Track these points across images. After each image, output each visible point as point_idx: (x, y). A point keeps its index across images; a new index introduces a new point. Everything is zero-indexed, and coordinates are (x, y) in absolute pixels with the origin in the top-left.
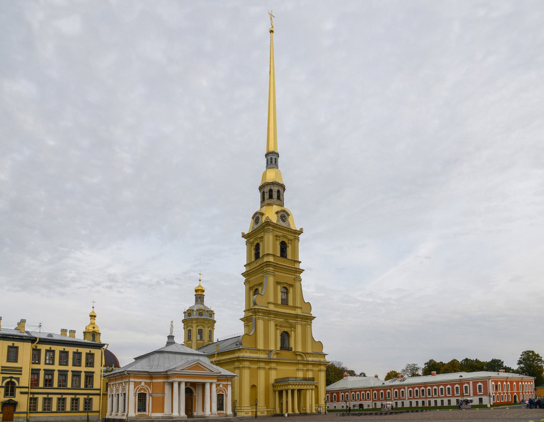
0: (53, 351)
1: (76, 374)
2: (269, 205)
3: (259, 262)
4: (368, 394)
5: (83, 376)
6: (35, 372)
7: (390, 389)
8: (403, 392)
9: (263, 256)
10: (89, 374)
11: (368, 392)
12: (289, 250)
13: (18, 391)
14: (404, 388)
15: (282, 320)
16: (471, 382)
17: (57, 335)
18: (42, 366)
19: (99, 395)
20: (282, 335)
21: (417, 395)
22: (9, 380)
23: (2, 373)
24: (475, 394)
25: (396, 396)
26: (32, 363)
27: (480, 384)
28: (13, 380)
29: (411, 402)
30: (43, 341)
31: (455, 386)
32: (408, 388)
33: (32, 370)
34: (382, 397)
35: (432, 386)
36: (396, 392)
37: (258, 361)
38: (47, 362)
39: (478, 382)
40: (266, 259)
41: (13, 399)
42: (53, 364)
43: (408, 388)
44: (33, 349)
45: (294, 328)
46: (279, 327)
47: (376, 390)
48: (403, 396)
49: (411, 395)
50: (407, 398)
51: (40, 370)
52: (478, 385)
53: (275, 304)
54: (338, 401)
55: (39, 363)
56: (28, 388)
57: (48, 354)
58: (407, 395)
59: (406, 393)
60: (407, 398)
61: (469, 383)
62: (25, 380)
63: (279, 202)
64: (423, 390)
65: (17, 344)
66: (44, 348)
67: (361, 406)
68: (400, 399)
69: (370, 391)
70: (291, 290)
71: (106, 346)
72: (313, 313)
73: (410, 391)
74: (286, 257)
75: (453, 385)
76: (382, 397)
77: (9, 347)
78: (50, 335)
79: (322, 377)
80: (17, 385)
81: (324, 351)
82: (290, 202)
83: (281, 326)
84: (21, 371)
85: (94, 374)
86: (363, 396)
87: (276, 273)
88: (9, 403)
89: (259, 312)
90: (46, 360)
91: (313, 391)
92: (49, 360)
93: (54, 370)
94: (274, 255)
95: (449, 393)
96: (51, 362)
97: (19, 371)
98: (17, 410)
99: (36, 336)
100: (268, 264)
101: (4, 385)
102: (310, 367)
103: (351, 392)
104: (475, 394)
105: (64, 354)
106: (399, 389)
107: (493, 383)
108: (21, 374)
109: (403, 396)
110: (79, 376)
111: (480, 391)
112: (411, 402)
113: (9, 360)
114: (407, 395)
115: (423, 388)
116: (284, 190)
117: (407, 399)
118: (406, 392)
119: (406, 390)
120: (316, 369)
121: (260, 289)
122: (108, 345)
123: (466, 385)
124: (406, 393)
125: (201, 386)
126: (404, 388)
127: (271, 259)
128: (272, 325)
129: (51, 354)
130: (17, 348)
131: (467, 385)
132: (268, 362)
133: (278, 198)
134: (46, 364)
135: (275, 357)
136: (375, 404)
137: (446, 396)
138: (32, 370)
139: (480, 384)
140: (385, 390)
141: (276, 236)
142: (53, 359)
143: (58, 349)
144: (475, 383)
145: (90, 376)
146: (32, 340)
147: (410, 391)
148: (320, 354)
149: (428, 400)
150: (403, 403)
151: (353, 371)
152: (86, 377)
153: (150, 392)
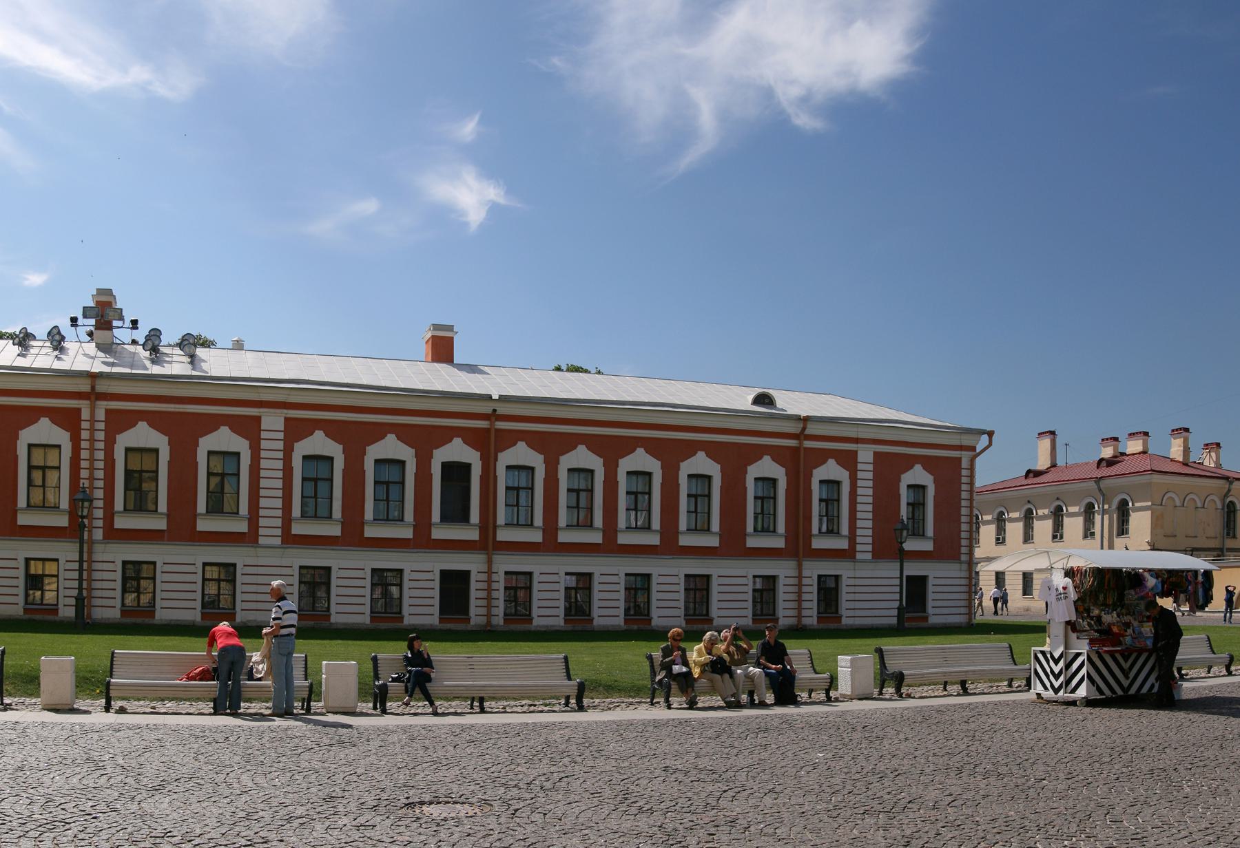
16: (865, 455)
27: (918, 475)
39: (908, 462)
49: (315, 508)
59: (271, 483)
61: (848, 461)
64: (456, 473)
68: (182, 529)
114: (271, 503)
115: (457, 451)
118: (271, 464)
123: (832, 470)
124: (271, 483)
131: (841, 474)
139: (918, 475)
144: (889, 466)
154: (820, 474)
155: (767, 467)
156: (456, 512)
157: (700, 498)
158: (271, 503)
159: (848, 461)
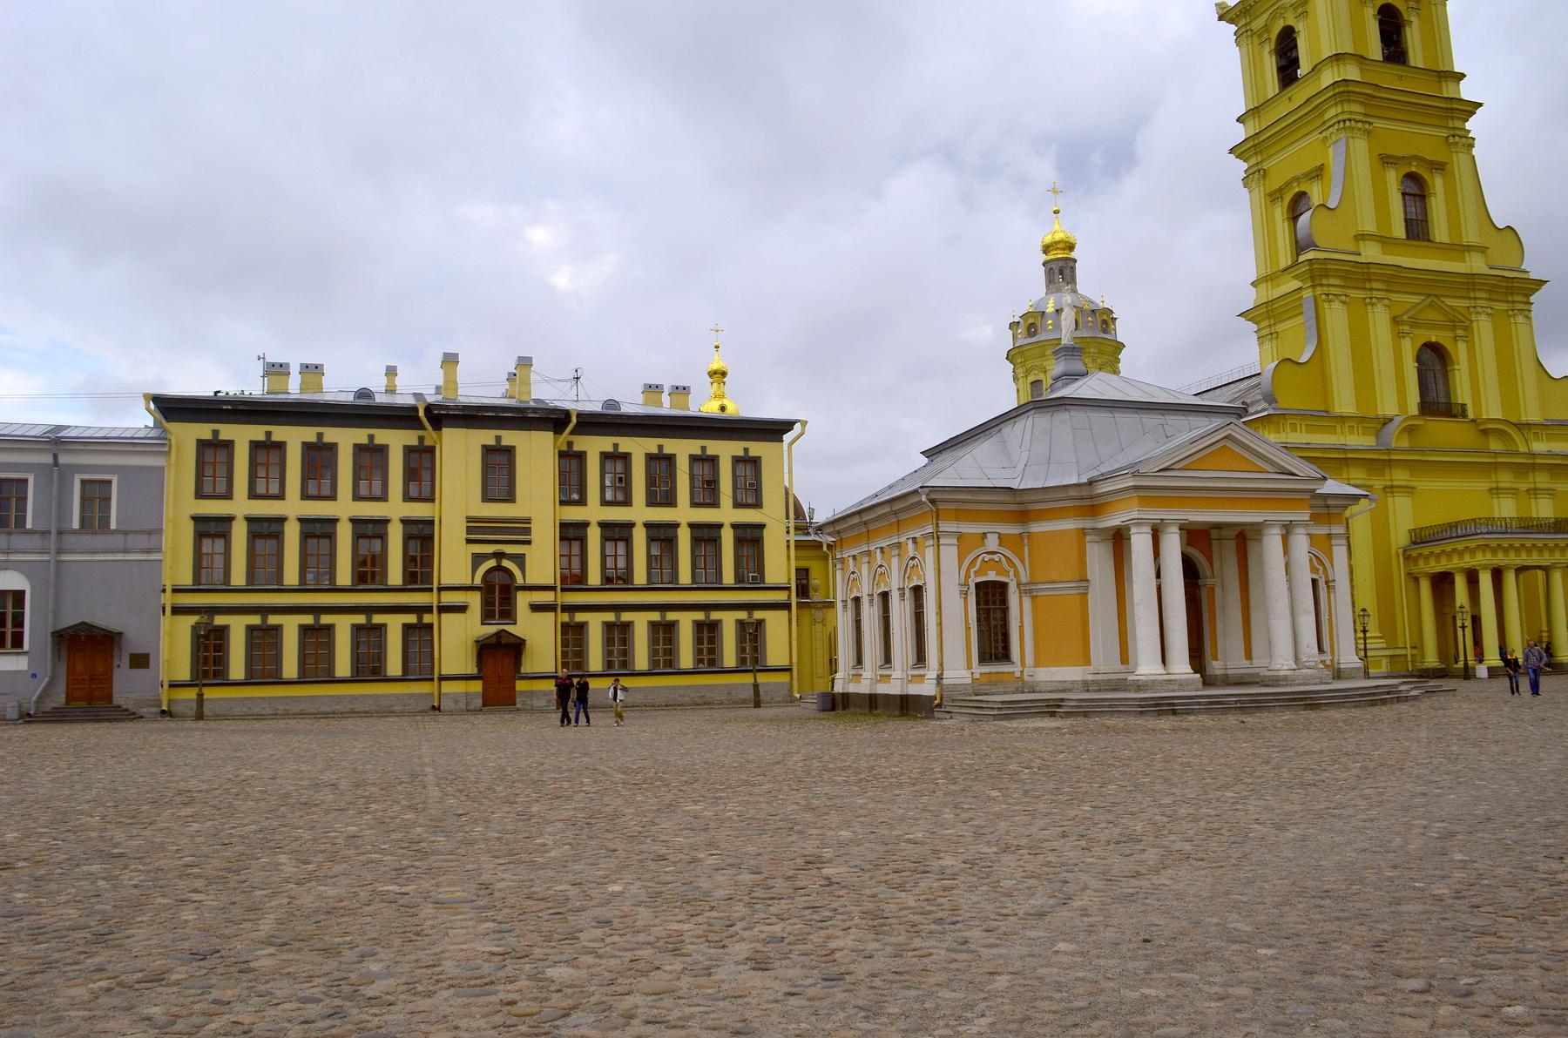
0: (626, 457)
1: (706, 535)
6: (571, 533)
13: (523, 600)
15: (1416, 299)
17: (633, 404)
18: (593, 512)
22: (492, 563)
23: (469, 541)
26: (562, 503)
28: (506, 563)
38: (609, 496)
41: (509, 628)
42: (627, 502)
45: (1466, 329)
51: (586, 525)
55: (582, 502)
56: (552, 588)
57: (609, 465)
66: (594, 446)
71: (797, 427)
72: (1534, 267)
78: (611, 403)
80: (520, 580)
83: (1414, 324)
84: (528, 531)
85: (766, 533)
88: (499, 642)
90: (603, 488)
92: (614, 486)
93: (632, 525)
96: (620, 497)
97: (520, 530)
101: (478, 581)
105: (661, 464)
108: (529, 542)
110: (716, 541)
113: (487, 498)
122: (804, 423)
125: (1230, 547)
129: (619, 467)
134: (604, 503)
138: (562, 525)
142: (624, 484)
143: (639, 448)
152: (739, 541)
153: (1024, 580)
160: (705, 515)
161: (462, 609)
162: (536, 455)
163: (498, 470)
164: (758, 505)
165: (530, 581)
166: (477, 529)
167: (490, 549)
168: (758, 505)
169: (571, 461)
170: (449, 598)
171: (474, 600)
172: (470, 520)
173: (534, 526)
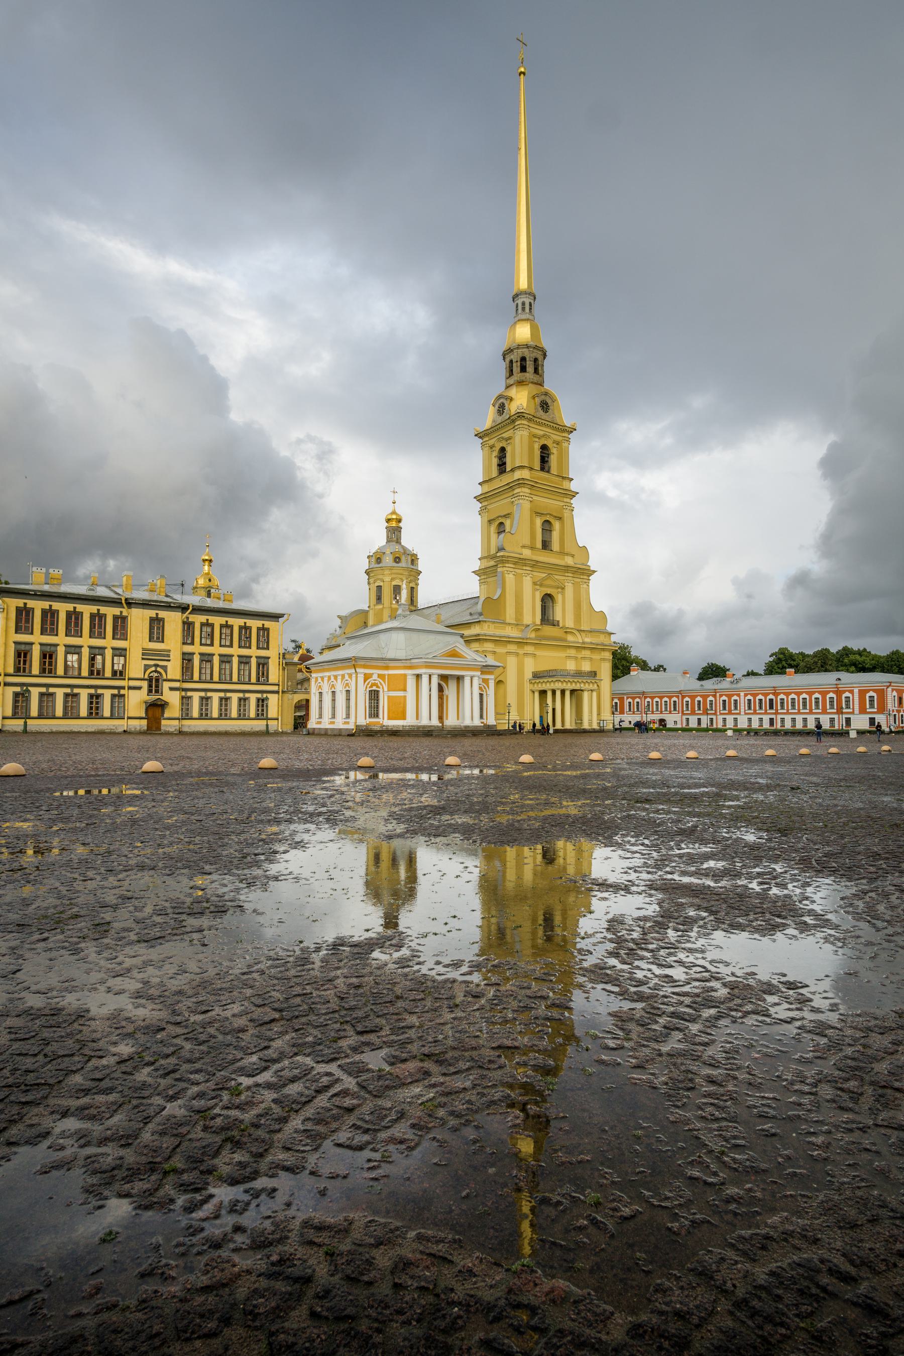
1: (244, 661)
2: (520, 383)
3: (506, 479)
4: (675, 702)
5: (254, 662)
7: (715, 696)
8: (736, 701)
9: (512, 470)
10: (262, 661)
11: (675, 699)
12: (553, 460)
13: (166, 685)
14: (739, 695)
16: (856, 691)
18: (196, 649)
19: (277, 692)
20: (543, 600)
21: (761, 708)
22: (153, 669)
23: (143, 659)
24: (863, 711)
25: (724, 708)
27: (872, 694)
28: (159, 669)
29: (750, 720)
30: (198, 610)
31: (828, 696)
32: (746, 695)
33: (184, 654)
34: (699, 709)
35: (787, 694)
36: (724, 701)
37: (508, 641)
38: (203, 641)
39: (869, 691)
40: (518, 475)
42: (212, 645)
43: (746, 695)
44: (184, 623)
46: (538, 587)
47: (689, 696)
48: (736, 708)
49: (750, 708)
50: (742, 711)
52: (868, 695)
53: (532, 548)
54: (622, 712)
55: (192, 643)
56: (179, 681)
58: (743, 706)
59: (742, 704)
60: (742, 711)
61: (852, 692)
62: (174, 669)
63: (536, 378)
64: (771, 700)
65: (162, 614)
67: (662, 722)
68: (730, 713)
69: (678, 697)
70: (557, 525)
72: (592, 564)
73: (749, 700)
74: (548, 472)
75: (824, 694)
76: (699, 709)
77: (152, 620)
79: (606, 670)
81: (609, 628)
82: (554, 377)
86: (666, 705)
87: (535, 498)
89: (508, 562)
90: (201, 638)
91: (595, 694)
94: (531, 469)
95: (817, 707)
96: (209, 642)
97: (165, 655)
98: (166, 716)
99: (188, 602)
100: (521, 483)
101: (146, 677)
102: (587, 653)
103: (646, 698)
104: (863, 711)
106: (730, 696)
107: (895, 693)
109: (736, 708)
111: (872, 706)
112: (750, 720)
113: (151, 639)
114: (742, 708)
116: (545, 356)
117: (742, 713)
118: (742, 701)
119: (742, 698)
120: (596, 656)
121: (507, 523)
124: (742, 704)
126: (739, 695)
127: (525, 474)
128: (527, 582)
130: (163, 620)
131: (850, 695)
132: (521, 643)
133: (536, 371)
135: (533, 635)
136: (688, 719)
137: (811, 712)
139: (872, 694)
140: (705, 697)
141: (535, 436)
144: (862, 693)
145: (263, 663)
146: (184, 608)
147: (749, 700)
148: (603, 633)
149: (779, 717)
150: (736, 720)
151: (644, 662)
154: (844, 695)
155: (831, 695)
156: (771, 707)
157: (832, 702)
158: (742, 708)
159: (852, 692)
160: (245, 652)
161: (139, 688)
162: (173, 621)
163: (156, 628)
164: (268, 648)
165: (169, 677)
166: (146, 654)
167: (152, 663)
168: (268, 648)
169: (188, 626)
170: (133, 683)
171: (145, 684)
172: (143, 649)
173: (171, 653)
